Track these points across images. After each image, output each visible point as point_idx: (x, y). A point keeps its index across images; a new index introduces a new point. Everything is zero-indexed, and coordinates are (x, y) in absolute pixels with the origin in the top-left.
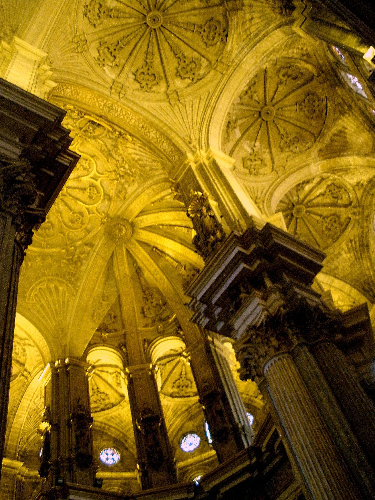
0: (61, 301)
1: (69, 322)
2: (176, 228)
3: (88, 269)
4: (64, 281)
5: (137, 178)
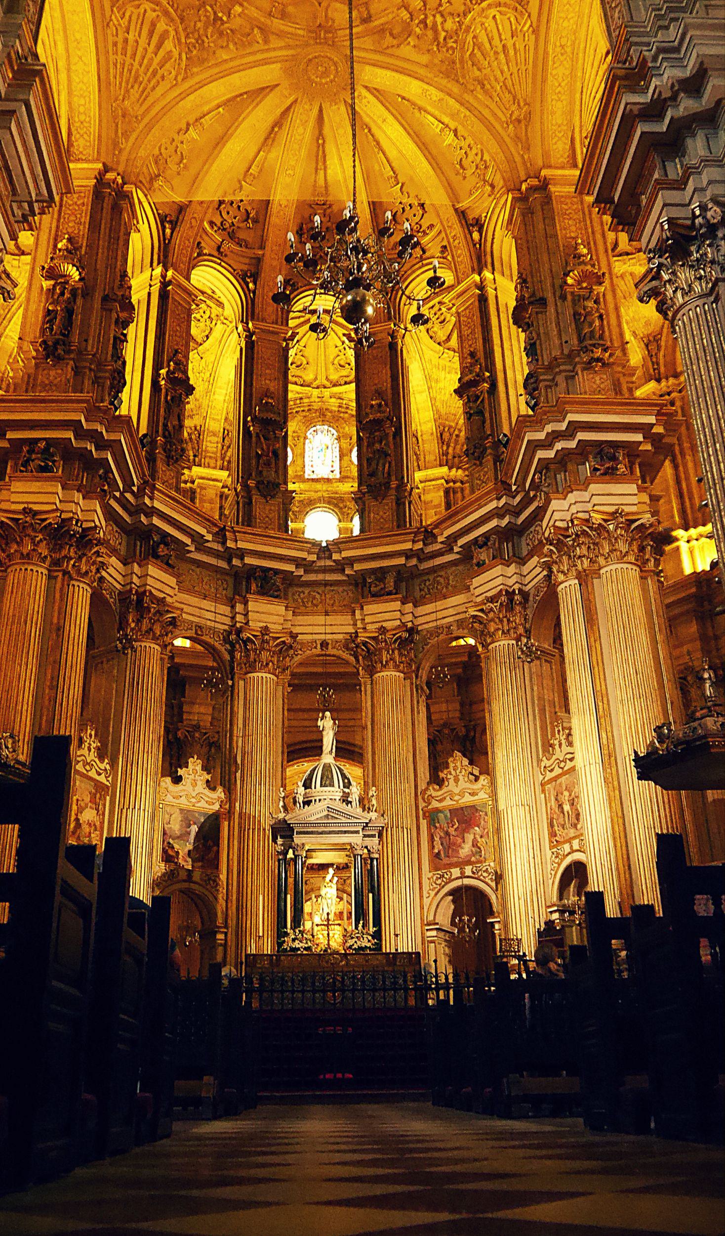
0: (155, 65)
1: (143, 115)
2: (381, 154)
3: (227, 66)
4: (183, 41)
5: (440, 56)
